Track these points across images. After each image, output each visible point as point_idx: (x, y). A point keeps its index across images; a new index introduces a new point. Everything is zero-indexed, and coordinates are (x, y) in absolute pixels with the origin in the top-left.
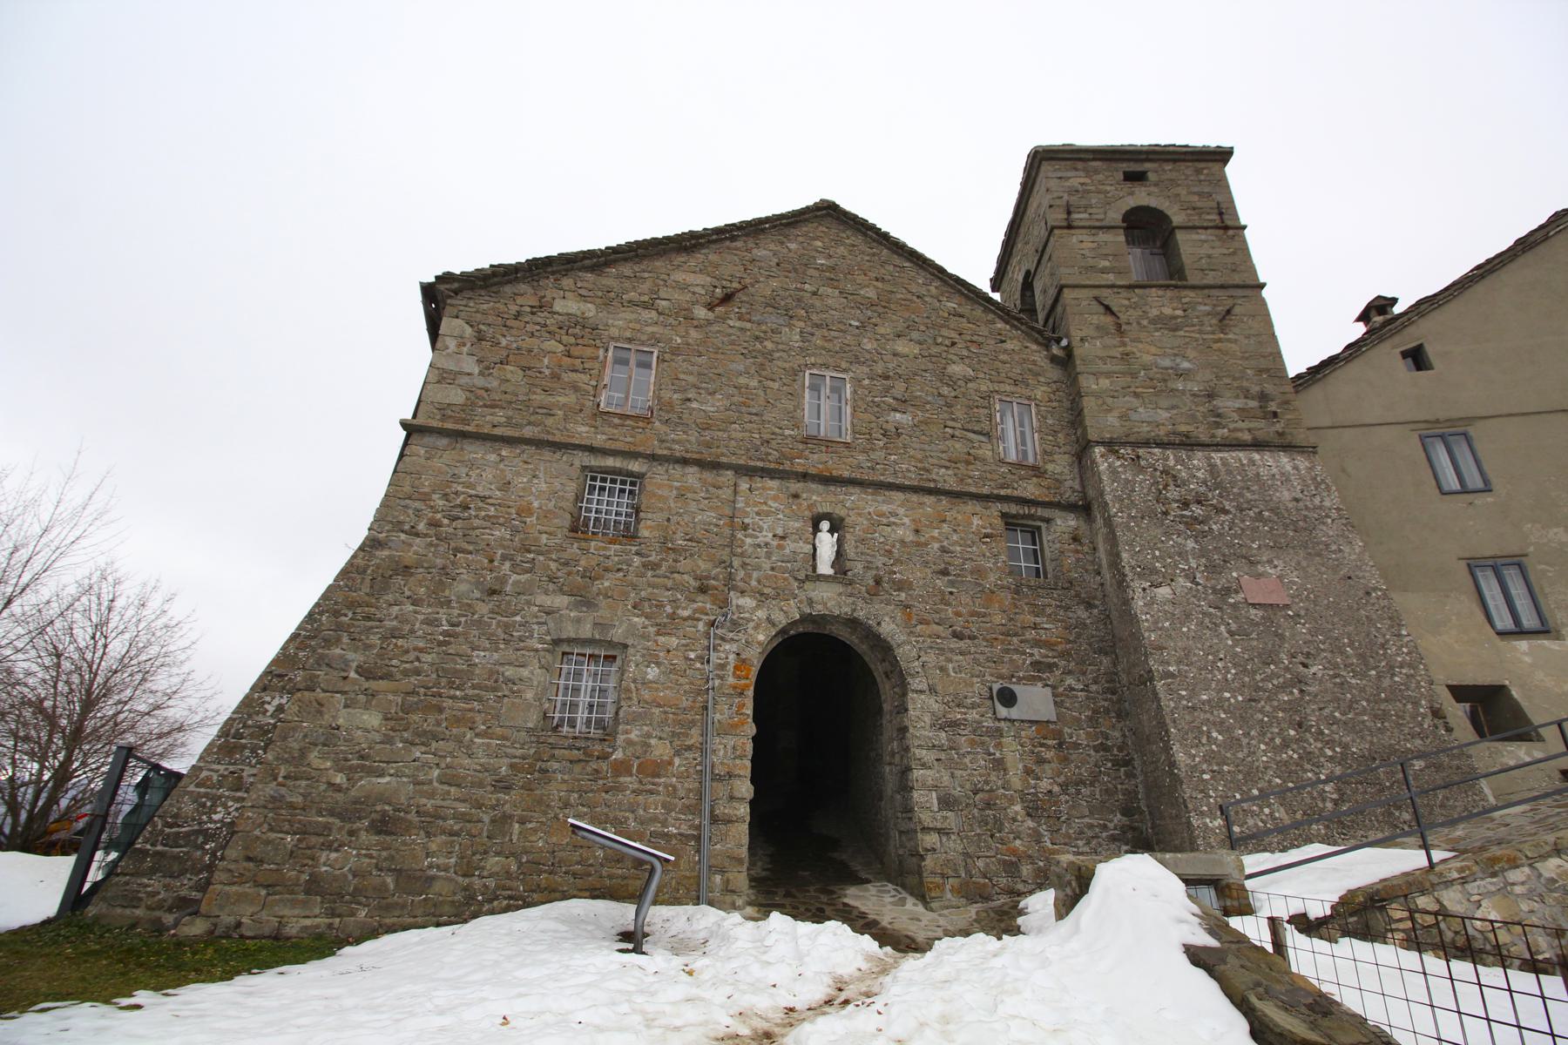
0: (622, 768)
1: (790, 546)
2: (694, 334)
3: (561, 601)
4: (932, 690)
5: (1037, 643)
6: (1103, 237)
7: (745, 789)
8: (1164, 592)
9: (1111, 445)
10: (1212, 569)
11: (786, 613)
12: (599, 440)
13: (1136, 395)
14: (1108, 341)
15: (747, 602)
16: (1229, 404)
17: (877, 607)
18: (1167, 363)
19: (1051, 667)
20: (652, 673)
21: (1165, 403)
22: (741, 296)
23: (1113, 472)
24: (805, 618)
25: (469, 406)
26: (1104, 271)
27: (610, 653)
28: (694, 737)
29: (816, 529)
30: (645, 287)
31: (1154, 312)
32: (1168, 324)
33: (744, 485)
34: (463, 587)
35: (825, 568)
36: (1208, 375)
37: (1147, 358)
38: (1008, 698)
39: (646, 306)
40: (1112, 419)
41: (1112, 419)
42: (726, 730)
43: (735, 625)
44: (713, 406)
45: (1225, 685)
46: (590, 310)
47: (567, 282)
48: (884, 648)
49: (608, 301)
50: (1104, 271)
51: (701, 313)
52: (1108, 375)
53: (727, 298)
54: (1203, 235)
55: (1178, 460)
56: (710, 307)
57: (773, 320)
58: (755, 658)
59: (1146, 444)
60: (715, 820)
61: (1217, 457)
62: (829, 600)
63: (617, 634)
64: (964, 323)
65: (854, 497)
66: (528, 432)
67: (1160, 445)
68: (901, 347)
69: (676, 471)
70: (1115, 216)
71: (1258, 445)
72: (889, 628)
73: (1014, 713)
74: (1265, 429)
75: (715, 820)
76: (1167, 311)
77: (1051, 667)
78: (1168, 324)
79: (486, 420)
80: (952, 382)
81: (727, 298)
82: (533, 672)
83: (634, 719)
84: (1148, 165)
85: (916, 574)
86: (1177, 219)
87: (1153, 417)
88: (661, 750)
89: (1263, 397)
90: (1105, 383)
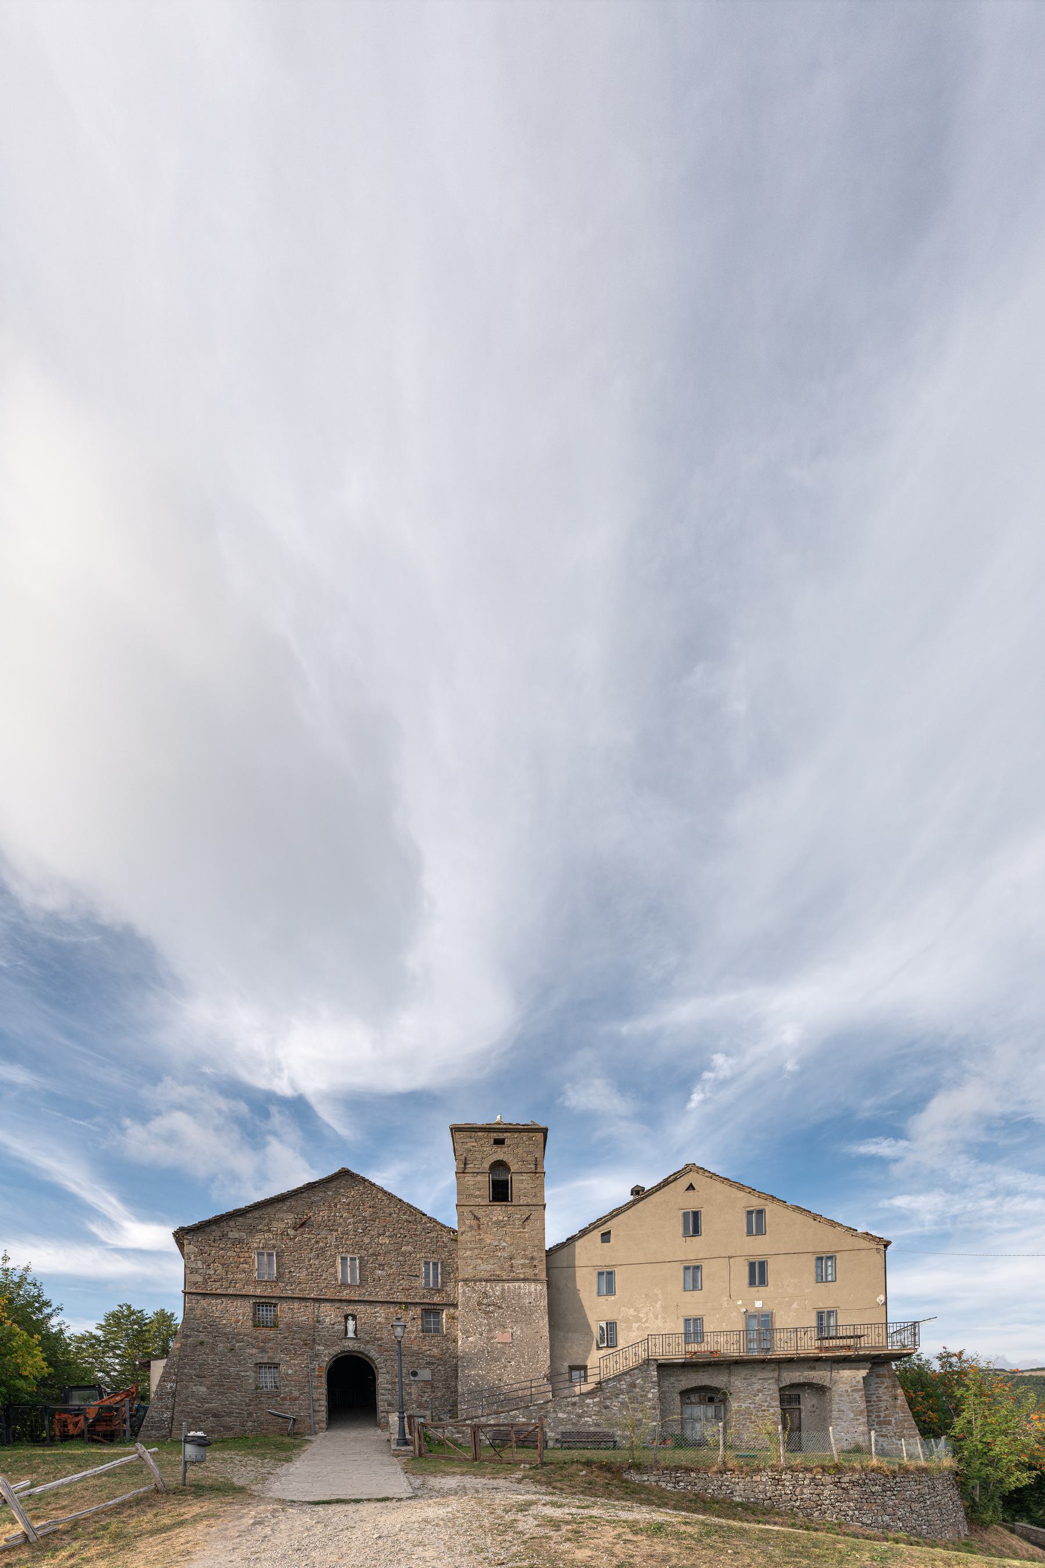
0: (284, 1399)
1: (336, 1327)
3: (255, 1351)
4: (388, 1373)
6: (479, 1178)
7: (324, 1403)
9: (465, 1280)
11: (336, 1350)
12: (258, 1292)
13: (482, 1259)
15: (321, 1348)
18: (496, 1243)
19: (433, 1364)
21: (491, 1262)
23: (464, 1292)
24: (342, 1352)
26: (476, 1197)
27: (276, 1366)
28: (306, 1390)
31: (495, 1219)
33: (317, 1305)
38: (415, 1374)
40: (469, 1269)
41: (469, 1269)
42: (316, 1388)
43: (317, 1355)
47: (232, 1223)
50: (476, 1197)
51: (291, 1232)
53: (303, 1225)
56: (295, 1229)
59: (480, 1280)
60: (314, 1411)
62: (350, 1345)
63: (276, 1361)
67: (487, 1281)
69: (290, 1303)
70: (486, 1165)
72: (373, 1354)
73: (416, 1379)
75: (314, 1411)
76: (501, 1218)
77: (433, 1364)
81: (303, 1225)
82: (250, 1373)
83: (286, 1386)
84: (505, 1135)
87: (485, 1268)
88: (296, 1394)
90: (468, 1253)
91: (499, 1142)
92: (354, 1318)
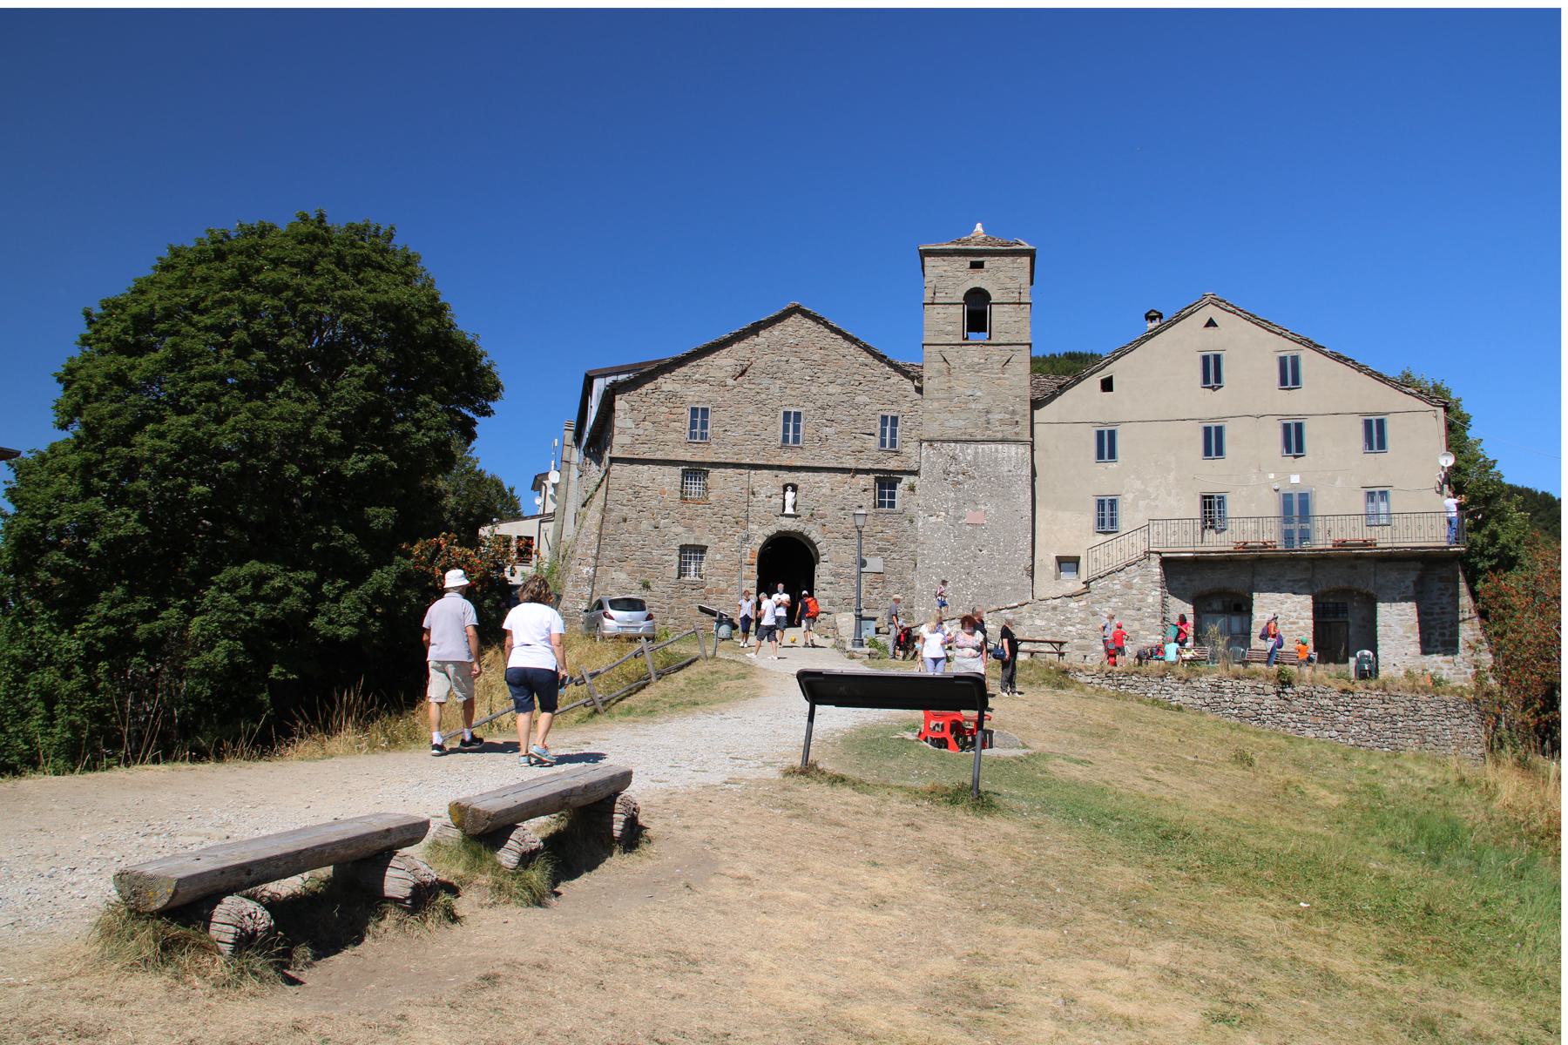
2: (727, 395)
3: (680, 529)
5: (882, 539)
6: (952, 309)
8: (933, 519)
10: (957, 508)
11: (771, 530)
14: (942, 379)
16: (994, 417)
17: (810, 527)
20: (718, 557)
21: (964, 416)
22: (750, 370)
23: (928, 456)
25: (633, 444)
28: (736, 580)
29: (785, 490)
30: (702, 370)
31: (969, 361)
32: (974, 368)
34: (645, 525)
35: (789, 510)
36: (989, 399)
37: (960, 390)
38: (863, 564)
39: (704, 382)
44: (737, 433)
45: (945, 558)
46: (677, 387)
48: (813, 545)
49: (687, 378)
51: (730, 382)
52: (938, 400)
53: (743, 373)
54: (1007, 308)
55: (962, 451)
57: (766, 382)
58: (757, 549)
59: (949, 441)
61: (980, 447)
62: (789, 525)
64: (868, 370)
65: (803, 475)
66: (659, 456)
67: (956, 441)
68: (832, 389)
70: (959, 296)
71: (1003, 441)
72: (815, 535)
74: (1009, 432)
78: (974, 368)
79: (642, 452)
80: (857, 407)
81: (743, 373)
85: (827, 510)
86: (995, 296)
87: (955, 424)
89: (1014, 412)
90: (936, 405)
91: (977, 266)
92: (795, 488)
